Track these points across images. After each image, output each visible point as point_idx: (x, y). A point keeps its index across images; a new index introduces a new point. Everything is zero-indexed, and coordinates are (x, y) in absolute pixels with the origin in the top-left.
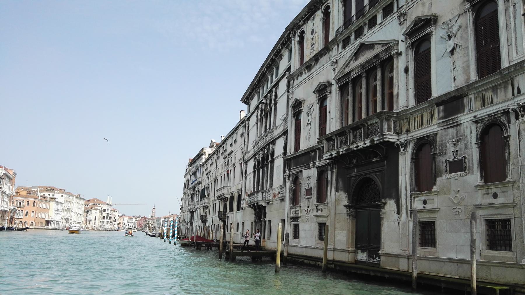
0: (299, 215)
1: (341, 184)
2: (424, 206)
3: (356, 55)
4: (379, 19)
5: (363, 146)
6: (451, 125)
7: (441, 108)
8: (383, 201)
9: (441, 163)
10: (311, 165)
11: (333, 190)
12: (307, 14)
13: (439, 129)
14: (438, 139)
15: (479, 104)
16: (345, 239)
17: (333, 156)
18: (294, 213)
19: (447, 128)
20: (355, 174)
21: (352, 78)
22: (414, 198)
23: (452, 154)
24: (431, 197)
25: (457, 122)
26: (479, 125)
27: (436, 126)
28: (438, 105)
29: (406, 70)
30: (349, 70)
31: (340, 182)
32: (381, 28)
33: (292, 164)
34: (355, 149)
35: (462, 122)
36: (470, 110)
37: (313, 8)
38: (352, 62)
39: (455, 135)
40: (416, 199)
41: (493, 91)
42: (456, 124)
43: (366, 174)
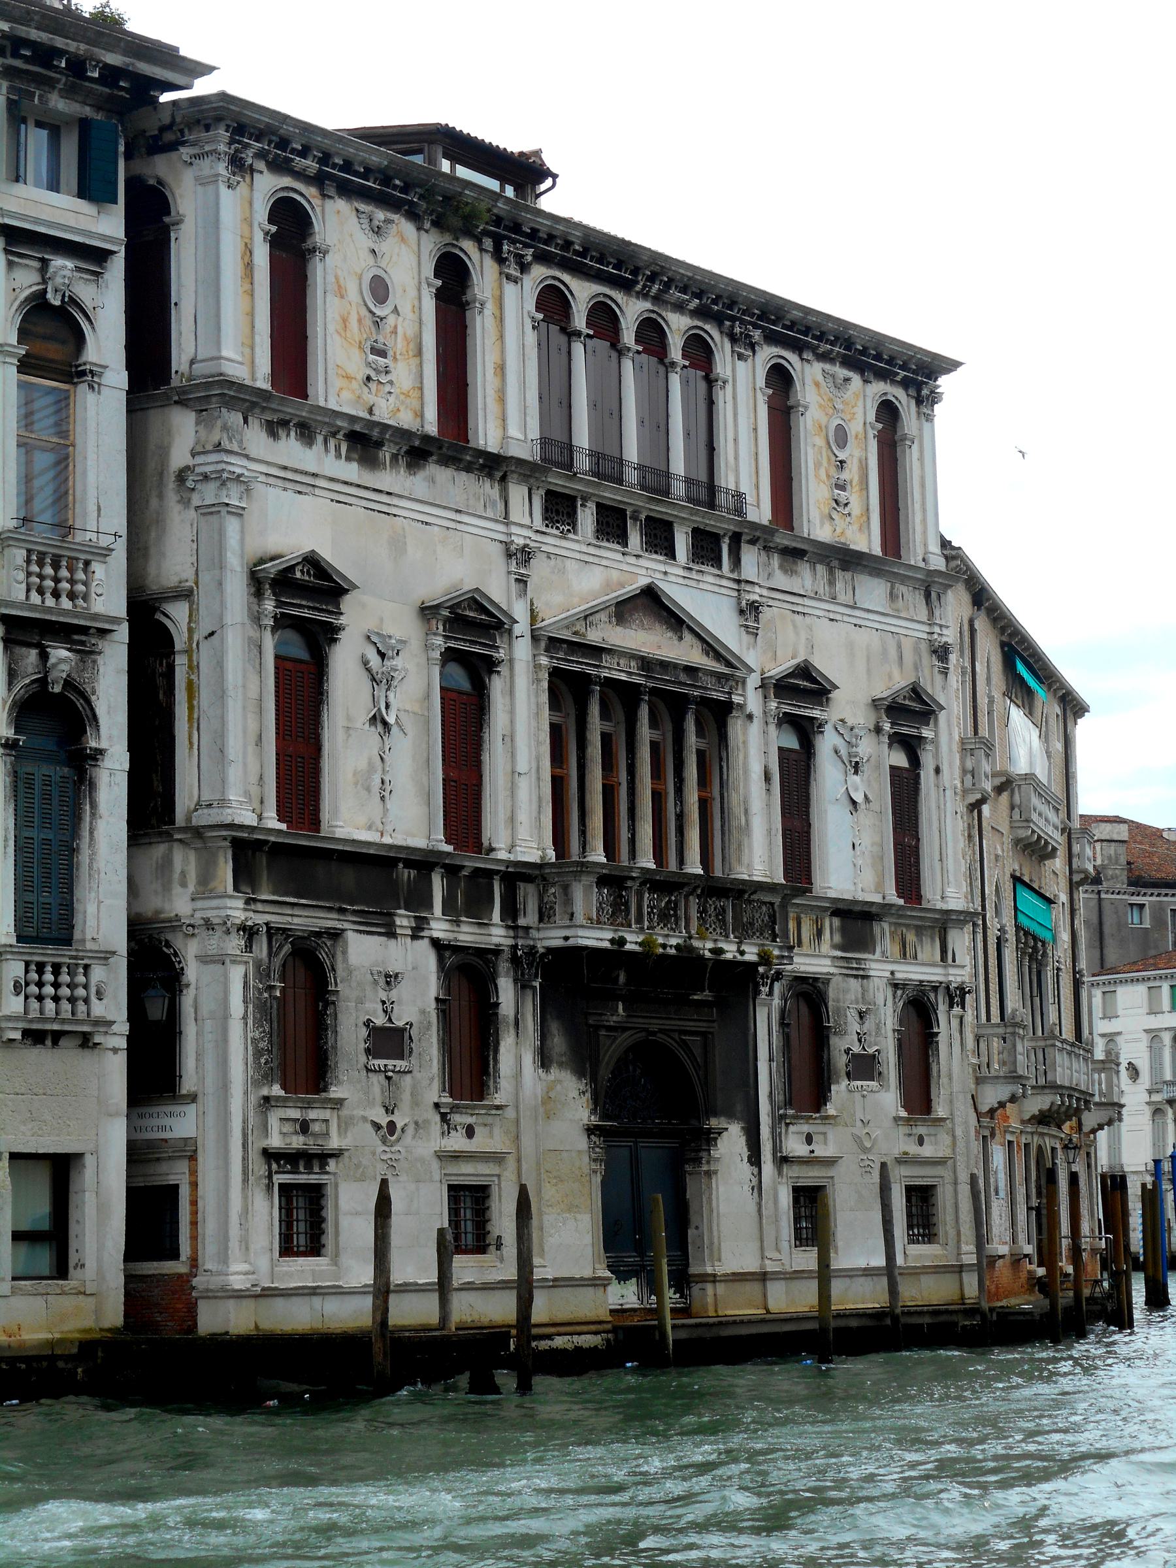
0: (334, 1143)
1: (558, 1043)
2: (811, 1148)
3: (623, 610)
4: (682, 542)
5: (735, 957)
6: (854, 972)
7: (836, 922)
8: (714, 1122)
9: (837, 1052)
10: (403, 920)
11: (528, 1059)
12: (356, 174)
13: (832, 970)
14: (832, 993)
15: (897, 949)
16: (588, 1239)
17: (628, 947)
19: (847, 975)
20: (619, 1019)
21: (605, 674)
22: (787, 1125)
23: (855, 1037)
24: (821, 1128)
25: (863, 969)
26: (899, 992)
27: (828, 962)
29: (767, 778)
30: (594, 636)
31: (555, 1032)
33: (265, 878)
34: (708, 954)
35: (872, 973)
36: (883, 952)
37: (395, 187)
38: (603, 616)
39: (860, 996)
40: (792, 1128)
41: (917, 935)
42: (861, 973)
43: (661, 1031)
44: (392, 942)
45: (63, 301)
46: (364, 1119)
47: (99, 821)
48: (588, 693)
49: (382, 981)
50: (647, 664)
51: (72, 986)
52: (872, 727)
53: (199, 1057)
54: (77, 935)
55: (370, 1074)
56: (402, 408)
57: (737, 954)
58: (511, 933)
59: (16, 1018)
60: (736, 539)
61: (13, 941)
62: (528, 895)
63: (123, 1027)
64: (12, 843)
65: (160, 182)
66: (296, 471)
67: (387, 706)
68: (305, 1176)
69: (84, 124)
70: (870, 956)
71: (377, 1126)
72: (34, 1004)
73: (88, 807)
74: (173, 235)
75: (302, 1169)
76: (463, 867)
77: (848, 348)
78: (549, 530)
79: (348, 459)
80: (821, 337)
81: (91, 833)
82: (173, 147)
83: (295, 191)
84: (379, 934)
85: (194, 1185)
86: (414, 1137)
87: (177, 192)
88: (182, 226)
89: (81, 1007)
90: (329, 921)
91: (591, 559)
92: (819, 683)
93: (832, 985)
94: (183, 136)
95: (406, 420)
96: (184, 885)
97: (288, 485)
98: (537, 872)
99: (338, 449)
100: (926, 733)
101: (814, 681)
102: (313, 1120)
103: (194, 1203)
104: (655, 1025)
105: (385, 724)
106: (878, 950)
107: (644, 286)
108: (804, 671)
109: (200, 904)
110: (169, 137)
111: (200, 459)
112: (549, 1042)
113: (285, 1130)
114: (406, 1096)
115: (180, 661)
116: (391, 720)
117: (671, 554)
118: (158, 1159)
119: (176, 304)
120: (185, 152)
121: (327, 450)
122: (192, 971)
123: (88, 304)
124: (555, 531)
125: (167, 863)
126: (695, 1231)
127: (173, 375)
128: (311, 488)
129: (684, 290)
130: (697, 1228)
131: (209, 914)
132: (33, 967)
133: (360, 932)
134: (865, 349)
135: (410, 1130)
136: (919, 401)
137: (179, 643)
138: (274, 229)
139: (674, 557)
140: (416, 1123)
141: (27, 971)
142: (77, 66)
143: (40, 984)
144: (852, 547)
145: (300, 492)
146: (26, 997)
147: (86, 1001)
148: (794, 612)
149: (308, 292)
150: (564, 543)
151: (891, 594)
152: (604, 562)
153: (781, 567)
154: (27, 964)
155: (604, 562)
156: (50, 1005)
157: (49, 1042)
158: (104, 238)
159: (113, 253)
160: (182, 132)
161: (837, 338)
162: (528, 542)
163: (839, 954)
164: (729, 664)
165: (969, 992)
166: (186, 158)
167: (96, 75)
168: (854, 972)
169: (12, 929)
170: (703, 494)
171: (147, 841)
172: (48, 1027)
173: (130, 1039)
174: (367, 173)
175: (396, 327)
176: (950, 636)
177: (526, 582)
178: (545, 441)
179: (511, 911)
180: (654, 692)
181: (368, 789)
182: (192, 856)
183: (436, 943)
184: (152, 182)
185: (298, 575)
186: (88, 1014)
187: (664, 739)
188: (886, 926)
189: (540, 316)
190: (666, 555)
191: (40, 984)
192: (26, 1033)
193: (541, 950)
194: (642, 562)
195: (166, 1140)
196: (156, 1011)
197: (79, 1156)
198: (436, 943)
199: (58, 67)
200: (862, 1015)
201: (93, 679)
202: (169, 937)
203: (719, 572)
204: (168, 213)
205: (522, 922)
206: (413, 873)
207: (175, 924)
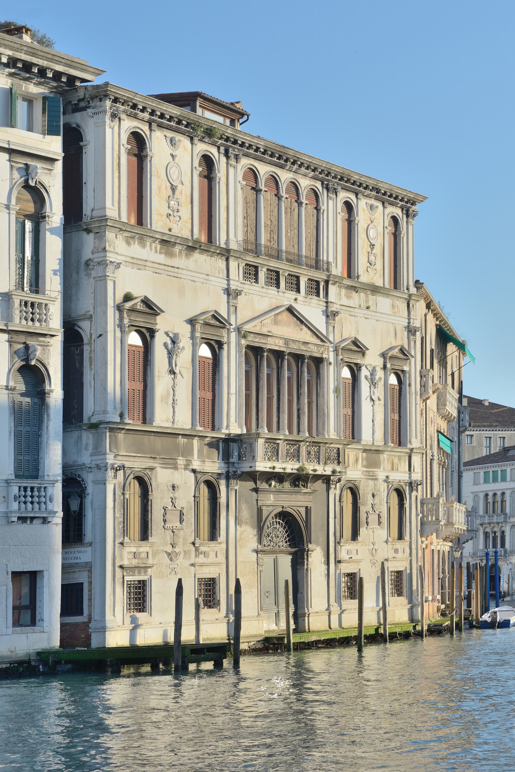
6: (371, 477)
10: (181, 461)
13: (362, 477)
15: (390, 466)
18: (131, 556)
20: (271, 502)
25: (375, 476)
27: (360, 473)
28: (365, 451)
31: (244, 509)
32: (305, 303)
35: (379, 477)
36: (384, 468)
42: (374, 477)
44: (176, 471)
45: (36, 184)
46: (163, 550)
47: (50, 422)
48: (262, 356)
49: (171, 488)
50: (287, 341)
51: (39, 497)
52: (382, 366)
53: (93, 526)
54: (40, 473)
55: (166, 531)
56: (184, 228)
57: (323, 472)
58: (227, 466)
59: (15, 512)
60: (327, 282)
61: (13, 477)
62: (234, 447)
63: (61, 514)
64: (13, 433)
65: (78, 126)
66: (138, 259)
67: (176, 365)
68: (138, 577)
69: (45, 99)
70: (378, 470)
71: (169, 554)
72: (23, 505)
73: (46, 416)
74: (84, 151)
75: (136, 574)
76: (207, 437)
77: (378, 193)
78: (246, 282)
79: (160, 253)
80: (366, 188)
81: (47, 428)
82: (84, 109)
83: (139, 128)
84: (171, 468)
85: (90, 583)
86: (184, 558)
87: (86, 130)
88: (88, 146)
89: (43, 506)
90: (150, 463)
91: (264, 295)
92: (360, 348)
93: (362, 483)
94: (89, 103)
95: (186, 234)
96: (86, 449)
97: (135, 266)
98: (238, 438)
99: (156, 248)
100: (406, 368)
101: (359, 347)
102: (142, 552)
103: (90, 591)
104: (286, 504)
105: (174, 373)
106: (382, 467)
107: (290, 167)
108: (355, 343)
109: (94, 458)
110: (83, 104)
111: (96, 255)
112: (241, 513)
113: (129, 557)
114: (181, 540)
115: (86, 348)
116: (177, 371)
117: (298, 291)
118: (74, 572)
119: (85, 183)
120: (89, 111)
121: (151, 249)
122: (90, 489)
123: (46, 184)
124: (249, 283)
125: (80, 438)
126: (301, 595)
127: (84, 216)
128: (144, 267)
129: (307, 168)
130: (301, 593)
131: (98, 462)
132: (22, 489)
133: (162, 467)
134: (385, 192)
135: (182, 555)
136: (408, 216)
137: (85, 341)
138: (129, 147)
139: (299, 292)
140: (185, 552)
141: (19, 491)
142: (42, 72)
143: (25, 496)
144: (376, 285)
145: (139, 269)
146: (19, 502)
147: (45, 503)
148: (350, 315)
149: (144, 175)
150: (253, 288)
151: (393, 305)
152: (270, 296)
153: (345, 295)
154: (20, 487)
155: (270, 296)
156: (29, 506)
157: (28, 522)
158: (55, 153)
159: (57, 160)
160: (89, 102)
161: (373, 188)
162: (237, 288)
163: (365, 469)
164: (322, 341)
165: (420, 484)
166: (91, 114)
167: (51, 76)
168: (371, 477)
169: (13, 472)
170: (313, 263)
171: (71, 430)
172: (29, 515)
173: (63, 519)
174: (171, 119)
175: (182, 191)
176: (417, 323)
177: (236, 308)
178: (246, 241)
179: (226, 457)
180: (290, 354)
181: (167, 404)
182: (91, 436)
183: (194, 471)
184: (74, 125)
185: (138, 307)
186: (46, 509)
187: (293, 376)
188: (385, 456)
189: (244, 183)
190: (296, 291)
191: (25, 496)
192: (19, 518)
193: (239, 472)
194: (286, 295)
195: (78, 563)
196: (74, 506)
197: (42, 571)
198: (194, 471)
199: (34, 72)
200: (373, 496)
201: (48, 358)
202: (80, 473)
203: (318, 298)
204: (82, 141)
205: (231, 460)
206: (186, 440)
207: (82, 467)
